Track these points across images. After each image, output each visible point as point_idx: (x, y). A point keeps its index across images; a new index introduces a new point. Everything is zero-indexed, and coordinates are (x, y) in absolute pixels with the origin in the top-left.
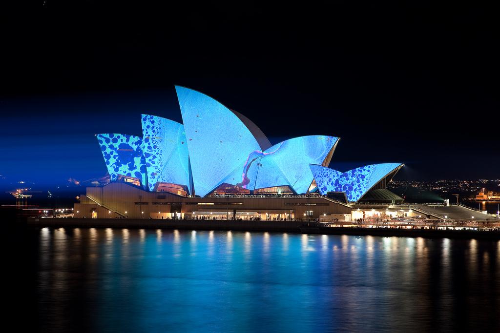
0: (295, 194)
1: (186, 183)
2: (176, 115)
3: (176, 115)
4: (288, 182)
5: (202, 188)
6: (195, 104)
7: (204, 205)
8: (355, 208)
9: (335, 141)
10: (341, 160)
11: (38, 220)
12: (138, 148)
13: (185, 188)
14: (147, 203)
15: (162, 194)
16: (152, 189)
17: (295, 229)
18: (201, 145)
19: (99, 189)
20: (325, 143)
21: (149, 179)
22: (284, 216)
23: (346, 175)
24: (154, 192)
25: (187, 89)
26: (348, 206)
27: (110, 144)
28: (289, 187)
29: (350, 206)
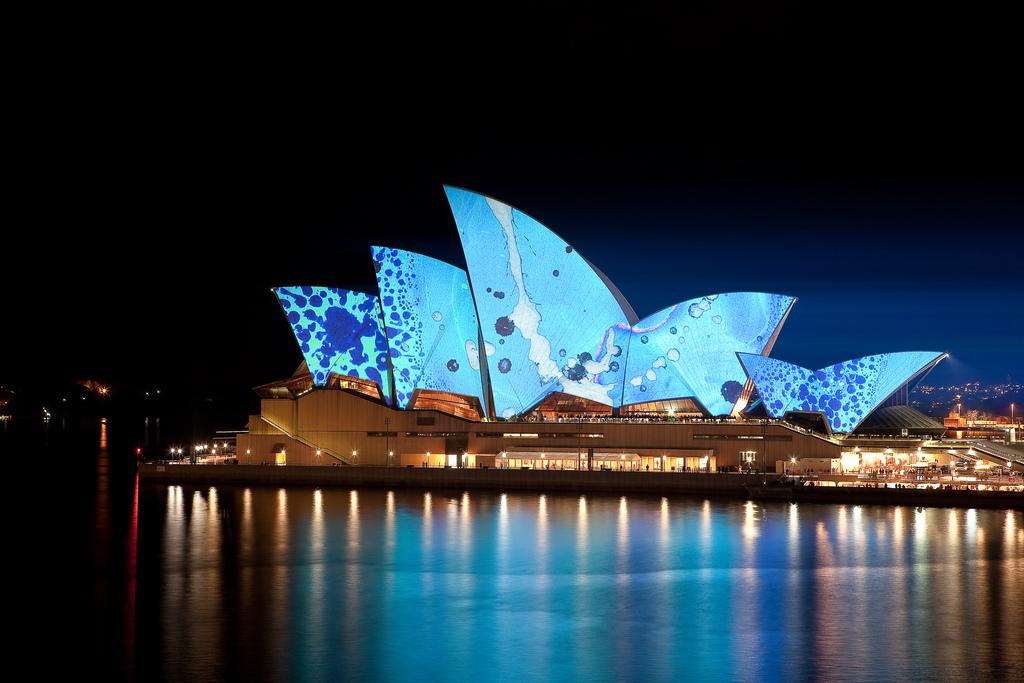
0: (707, 415)
1: (476, 390)
2: (450, 250)
3: (450, 250)
4: (689, 388)
5: (510, 402)
6: (491, 226)
7: (517, 439)
8: (848, 445)
9: (786, 302)
10: (795, 345)
11: (161, 469)
12: (367, 318)
13: (473, 402)
14: (395, 434)
15: (425, 415)
16: (403, 403)
17: (725, 492)
18: (502, 310)
19: (287, 403)
20: (765, 310)
21: (397, 383)
22: (701, 463)
23: (822, 377)
24: (409, 409)
25: (471, 195)
26: (833, 440)
27: (309, 309)
28: (694, 400)
29: (838, 443)
